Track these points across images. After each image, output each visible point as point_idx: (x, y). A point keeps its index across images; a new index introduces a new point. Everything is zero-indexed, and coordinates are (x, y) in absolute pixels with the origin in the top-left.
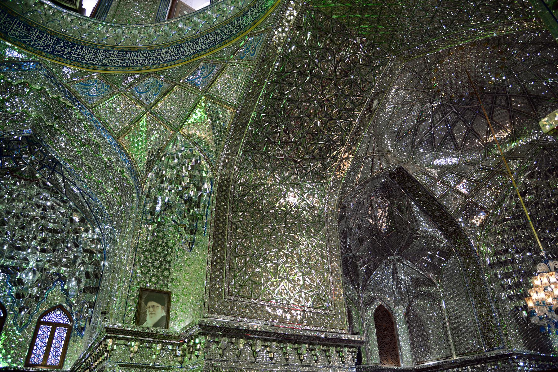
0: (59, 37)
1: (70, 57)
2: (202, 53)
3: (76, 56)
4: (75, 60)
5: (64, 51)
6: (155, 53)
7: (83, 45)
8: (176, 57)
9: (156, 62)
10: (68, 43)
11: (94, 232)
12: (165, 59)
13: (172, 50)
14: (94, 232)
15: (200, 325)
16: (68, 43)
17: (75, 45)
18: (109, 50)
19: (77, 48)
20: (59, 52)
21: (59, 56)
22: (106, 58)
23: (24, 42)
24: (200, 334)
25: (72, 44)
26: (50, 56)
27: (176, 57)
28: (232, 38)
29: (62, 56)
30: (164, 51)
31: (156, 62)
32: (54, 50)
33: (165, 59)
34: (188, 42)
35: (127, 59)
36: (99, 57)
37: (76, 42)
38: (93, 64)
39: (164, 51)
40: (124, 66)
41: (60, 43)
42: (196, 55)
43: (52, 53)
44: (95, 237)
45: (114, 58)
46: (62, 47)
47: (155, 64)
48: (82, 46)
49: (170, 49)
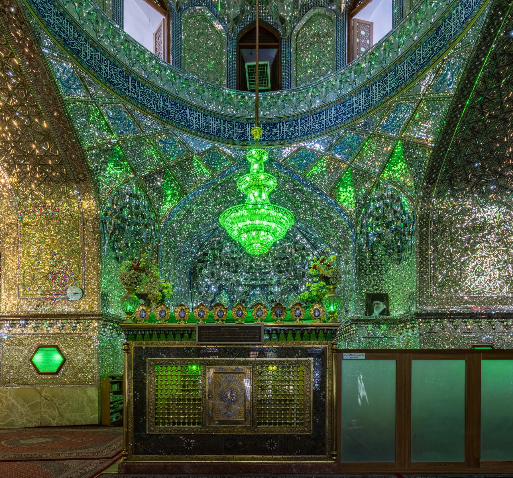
1: (277, 137)
2: (393, 93)
3: (281, 135)
4: (282, 139)
5: (271, 134)
6: (345, 105)
8: (367, 104)
9: (349, 116)
10: (272, 125)
12: (357, 110)
13: (361, 96)
16: (272, 125)
17: (277, 123)
19: (280, 127)
20: (269, 137)
21: (270, 140)
22: (304, 127)
23: (245, 140)
25: (275, 124)
27: (367, 104)
29: (271, 140)
30: (353, 100)
31: (349, 116)
32: (265, 137)
33: (357, 110)
34: (376, 83)
35: (322, 121)
36: (298, 128)
37: (277, 121)
38: (296, 137)
39: (353, 100)
40: (322, 130)
41: (266, 128)
42: (387, 98)
46: (269, 131)
47: (349, 118)
48: (283, 123)
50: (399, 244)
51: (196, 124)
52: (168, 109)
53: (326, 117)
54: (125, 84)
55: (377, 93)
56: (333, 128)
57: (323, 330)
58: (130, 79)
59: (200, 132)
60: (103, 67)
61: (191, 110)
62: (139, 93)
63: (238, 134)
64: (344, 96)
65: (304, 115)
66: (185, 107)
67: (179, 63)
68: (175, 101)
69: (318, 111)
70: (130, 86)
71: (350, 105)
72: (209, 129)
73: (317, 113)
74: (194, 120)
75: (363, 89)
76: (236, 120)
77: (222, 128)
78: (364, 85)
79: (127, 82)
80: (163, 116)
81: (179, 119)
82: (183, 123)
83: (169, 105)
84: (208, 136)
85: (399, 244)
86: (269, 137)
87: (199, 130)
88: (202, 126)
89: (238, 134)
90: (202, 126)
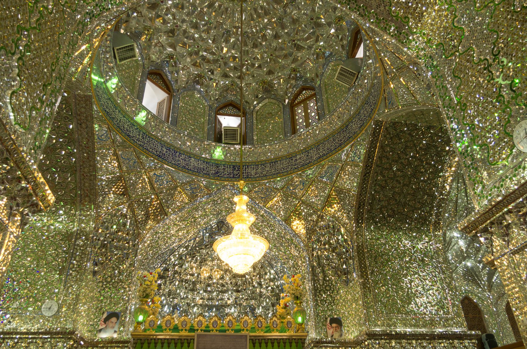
0: (234, 164)
2: (325, 157)
7: (248, 165)
9: (296, 167)
11: (270, 274)
14: (270, 274)
15: (367, 334)
18: (263, 164)
20: (237, 175)
24: (368, 339)
26: (234, 179)
28: (343, 146)
30: (298, 157)
31: (296, 167)
36: (259, 171)
39: (298, 157)
43: (233, 177)
44: (272, 276)
45: (268, 169)
49: (302, 155)
50: (344, 267)
51: (183, 163)
52: (164, 152)
53: (279, 166)
54: (138, 137)
55: (314, 154)
56: (285, 174)
57: (295, 339)
58: (141, 133)
59: (185, 169)
60: (126, 126)
61: (180, 153)
62: (146, 142)
63: (213, 172)
64: (291, 154)
65: (263, 162)
66: (175, 151)
67: (175, 122)
68: (169, 147)
69: (274, 161)
70: (141, 138)
71: (296, 160)
72: (192, 167)
73: (273, 162)
74: (181, 161)
75: (304, 151)
76: (213, 161)
77: (202, 166)
78: (305, 149)
79: (139, 135)
80: (161, 157)
81: (170, 159)
82: (173, 162)
83: (165, 150)
84: (191, 172)
85: (344, 267)
86: (237, 175)
87: (184, 167)
88: (187, 164)
89: (213, 172)
90: (187, 164)
